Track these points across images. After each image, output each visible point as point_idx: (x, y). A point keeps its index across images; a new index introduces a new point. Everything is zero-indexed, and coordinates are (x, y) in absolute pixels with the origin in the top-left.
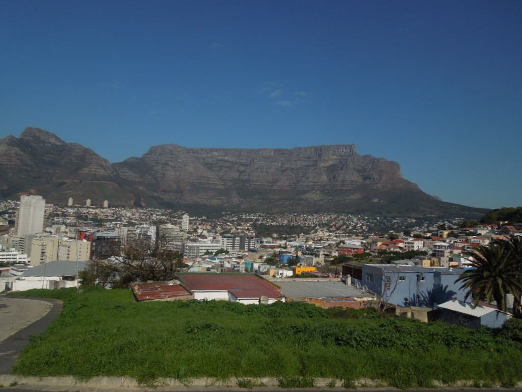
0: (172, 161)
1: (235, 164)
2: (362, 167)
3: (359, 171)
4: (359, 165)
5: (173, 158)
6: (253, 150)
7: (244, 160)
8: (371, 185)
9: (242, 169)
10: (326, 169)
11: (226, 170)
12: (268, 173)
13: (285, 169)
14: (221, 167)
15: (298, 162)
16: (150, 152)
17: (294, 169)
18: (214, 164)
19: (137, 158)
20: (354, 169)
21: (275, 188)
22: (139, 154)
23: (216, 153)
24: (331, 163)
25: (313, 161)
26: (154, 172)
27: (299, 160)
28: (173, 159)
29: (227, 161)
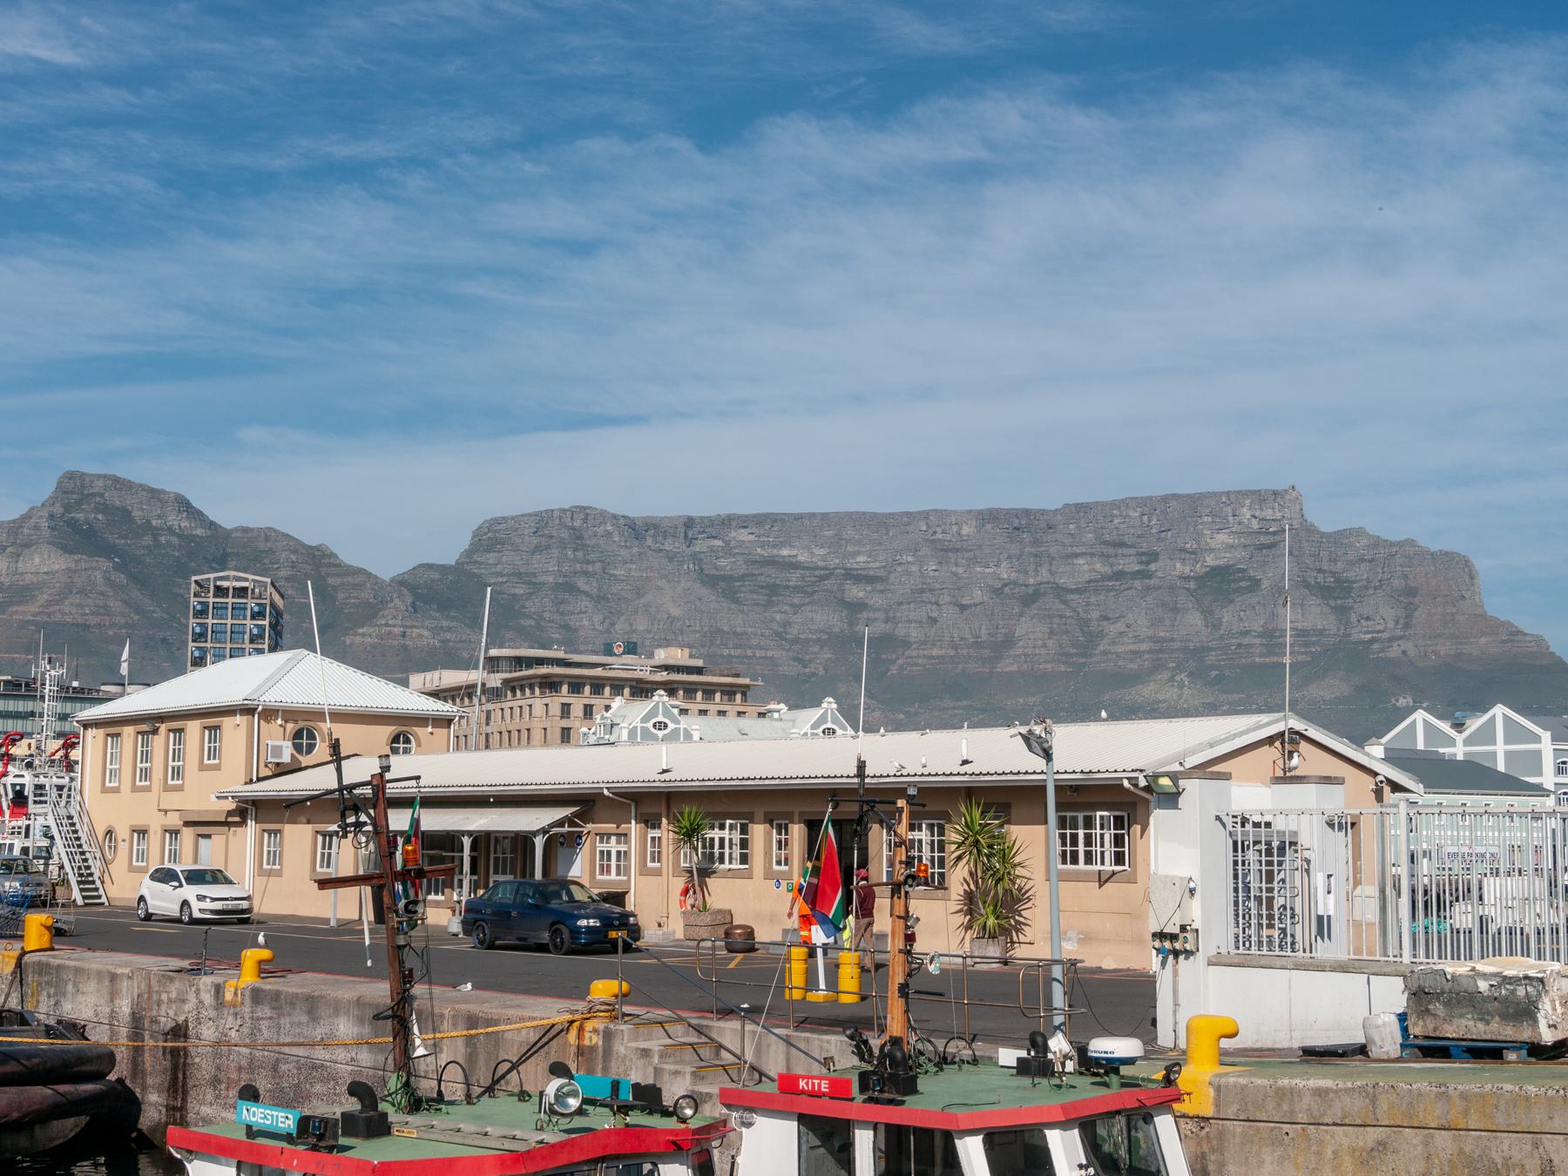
0: (585, 573)
1: (822, 578)
2: (1333, 573)
3: (1324, 592)
4: (1320, 571)
5: (588, 562)
6: (892, 515)
7: (861, 558)
8: (1376, 646)
9: (856, 592)
10: (1192, 585)
11: (796, 601)
12: (963, 608)
13: (1031, 591)
14: (773, 589)
15: (1080, 561)
16: (490, 537)
17: (1072, 591)
18: (741, 578)
19: (444, 569)
20: (1306, 584)
21: (1008, 666)
22: (450, 557)
23: (744, 535)
24: (1211, 561)
25: (1138, 554)
26: (533, 623)
27: (1084, 554)
28: (590, 568)
29: (796, 566)
